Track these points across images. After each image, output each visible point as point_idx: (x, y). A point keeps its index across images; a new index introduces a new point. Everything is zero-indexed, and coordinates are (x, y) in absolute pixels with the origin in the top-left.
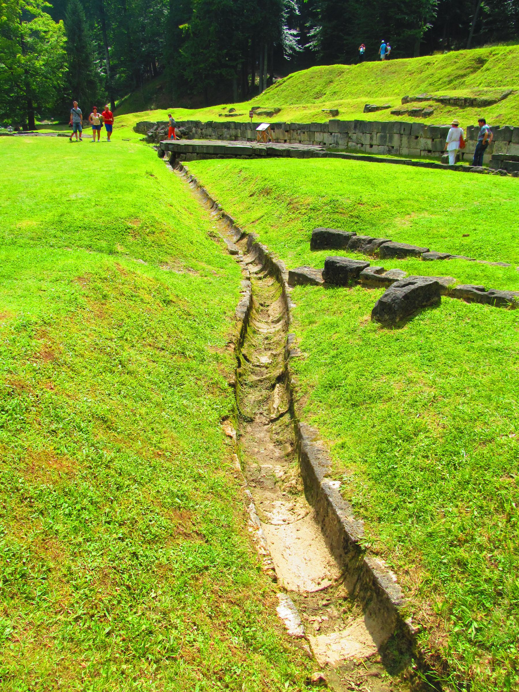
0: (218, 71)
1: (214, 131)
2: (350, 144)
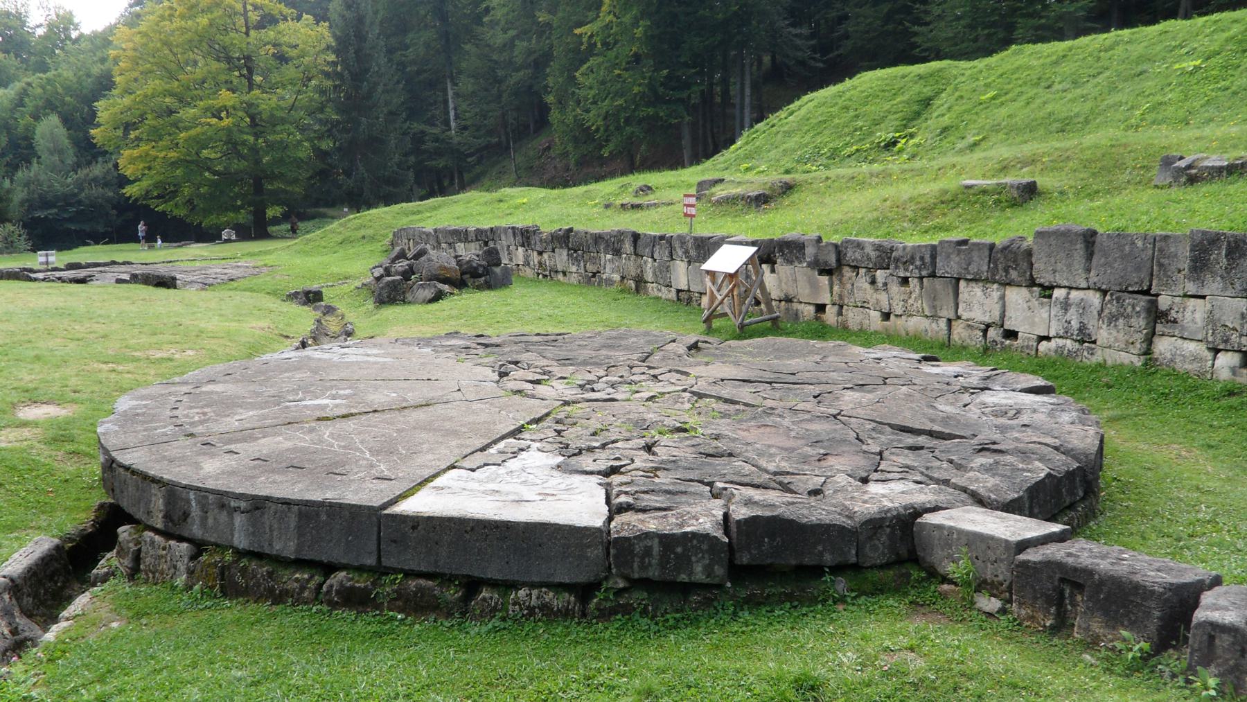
0: (651, 111)
1: (576, 261)
2: (1163, 346)
